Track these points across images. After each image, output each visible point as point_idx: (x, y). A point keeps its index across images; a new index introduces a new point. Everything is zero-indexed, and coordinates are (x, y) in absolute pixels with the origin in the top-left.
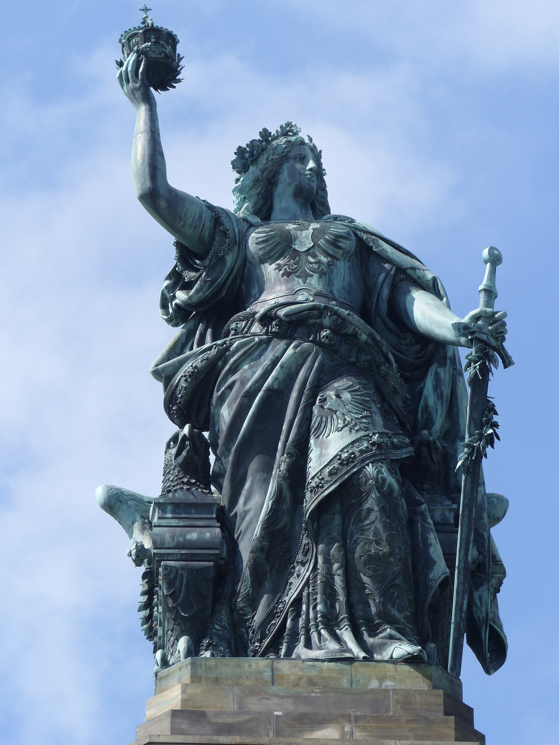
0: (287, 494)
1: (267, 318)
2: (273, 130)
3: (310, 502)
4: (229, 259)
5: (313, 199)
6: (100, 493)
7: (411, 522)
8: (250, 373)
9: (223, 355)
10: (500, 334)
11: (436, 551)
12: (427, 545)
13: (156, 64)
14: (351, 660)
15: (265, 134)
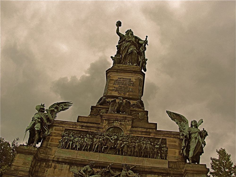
0: (126, 53)
1: (126, 41)
2: (129, 30)
3: (128, 53)
4: (124, 38)
5: (132, 34)
6: (110, 56)
7: (138, 57)
8: (124, 45)
9: (122, 44)
10: (147, 42)
11: (140, 59)
12: (139, 58)
13: (119, 24)
14: (130, 65)
15: (128, 30)
